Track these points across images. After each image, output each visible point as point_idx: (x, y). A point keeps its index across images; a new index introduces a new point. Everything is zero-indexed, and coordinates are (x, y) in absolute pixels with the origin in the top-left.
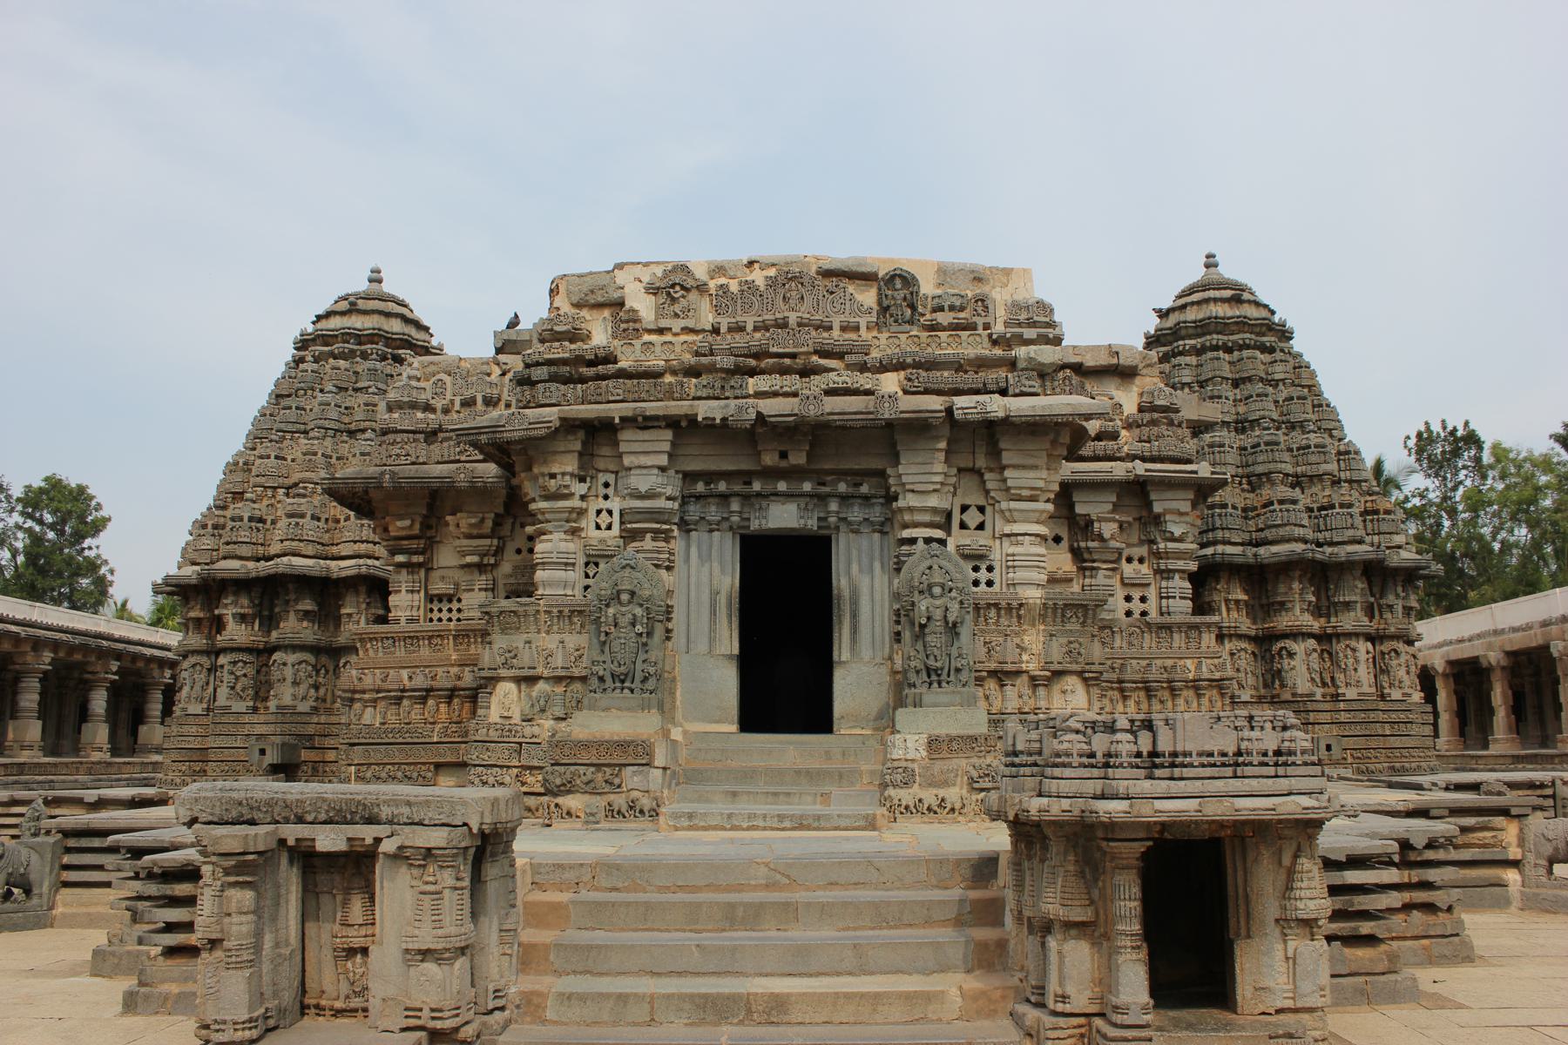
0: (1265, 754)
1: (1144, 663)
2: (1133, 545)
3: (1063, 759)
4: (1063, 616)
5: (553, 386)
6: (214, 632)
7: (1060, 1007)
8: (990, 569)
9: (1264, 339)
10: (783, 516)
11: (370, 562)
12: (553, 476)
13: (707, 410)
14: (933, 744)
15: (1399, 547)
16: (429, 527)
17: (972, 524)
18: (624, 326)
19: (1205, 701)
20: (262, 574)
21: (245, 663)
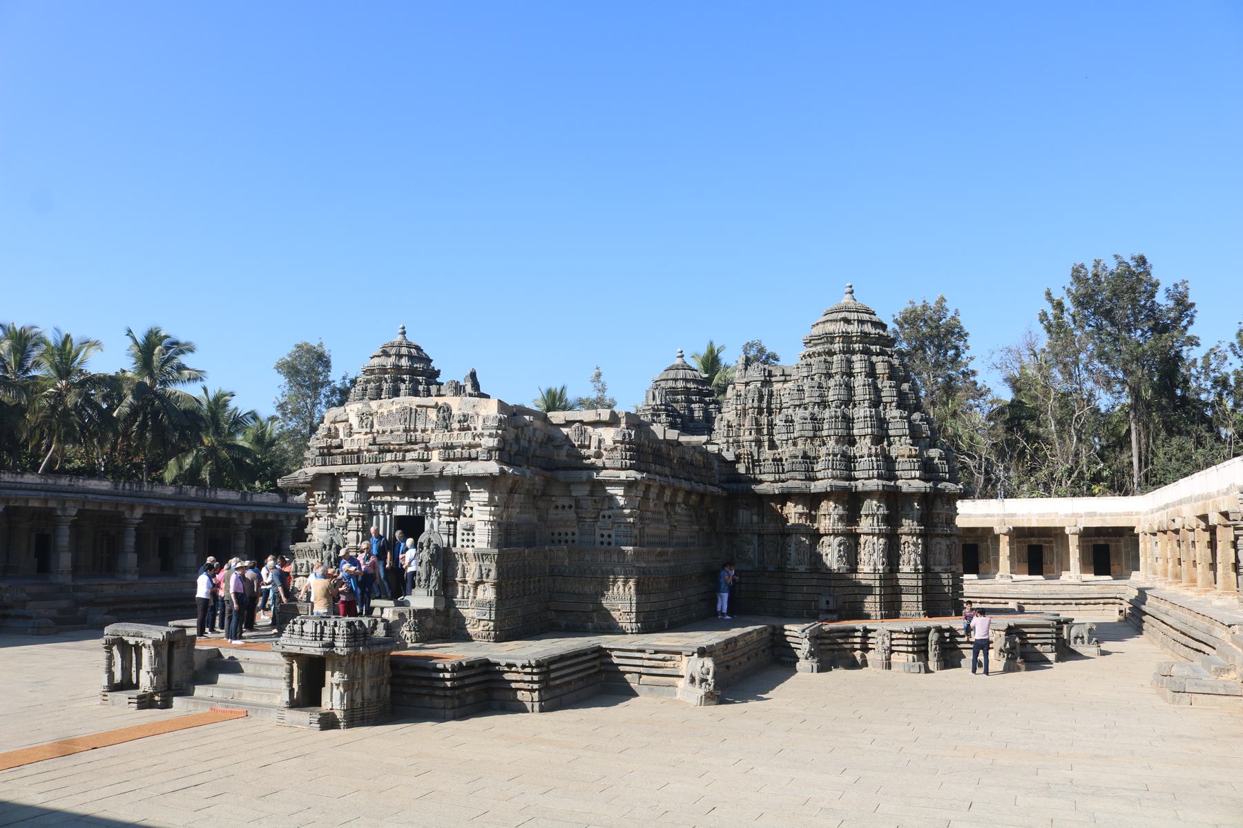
2: (604, 510)
4: (483, 559)
5: (320, 458)
8: (474, 534)
9: (857, 345)
10: (401, 511)
12: (319, 495)
17: (468, 515)
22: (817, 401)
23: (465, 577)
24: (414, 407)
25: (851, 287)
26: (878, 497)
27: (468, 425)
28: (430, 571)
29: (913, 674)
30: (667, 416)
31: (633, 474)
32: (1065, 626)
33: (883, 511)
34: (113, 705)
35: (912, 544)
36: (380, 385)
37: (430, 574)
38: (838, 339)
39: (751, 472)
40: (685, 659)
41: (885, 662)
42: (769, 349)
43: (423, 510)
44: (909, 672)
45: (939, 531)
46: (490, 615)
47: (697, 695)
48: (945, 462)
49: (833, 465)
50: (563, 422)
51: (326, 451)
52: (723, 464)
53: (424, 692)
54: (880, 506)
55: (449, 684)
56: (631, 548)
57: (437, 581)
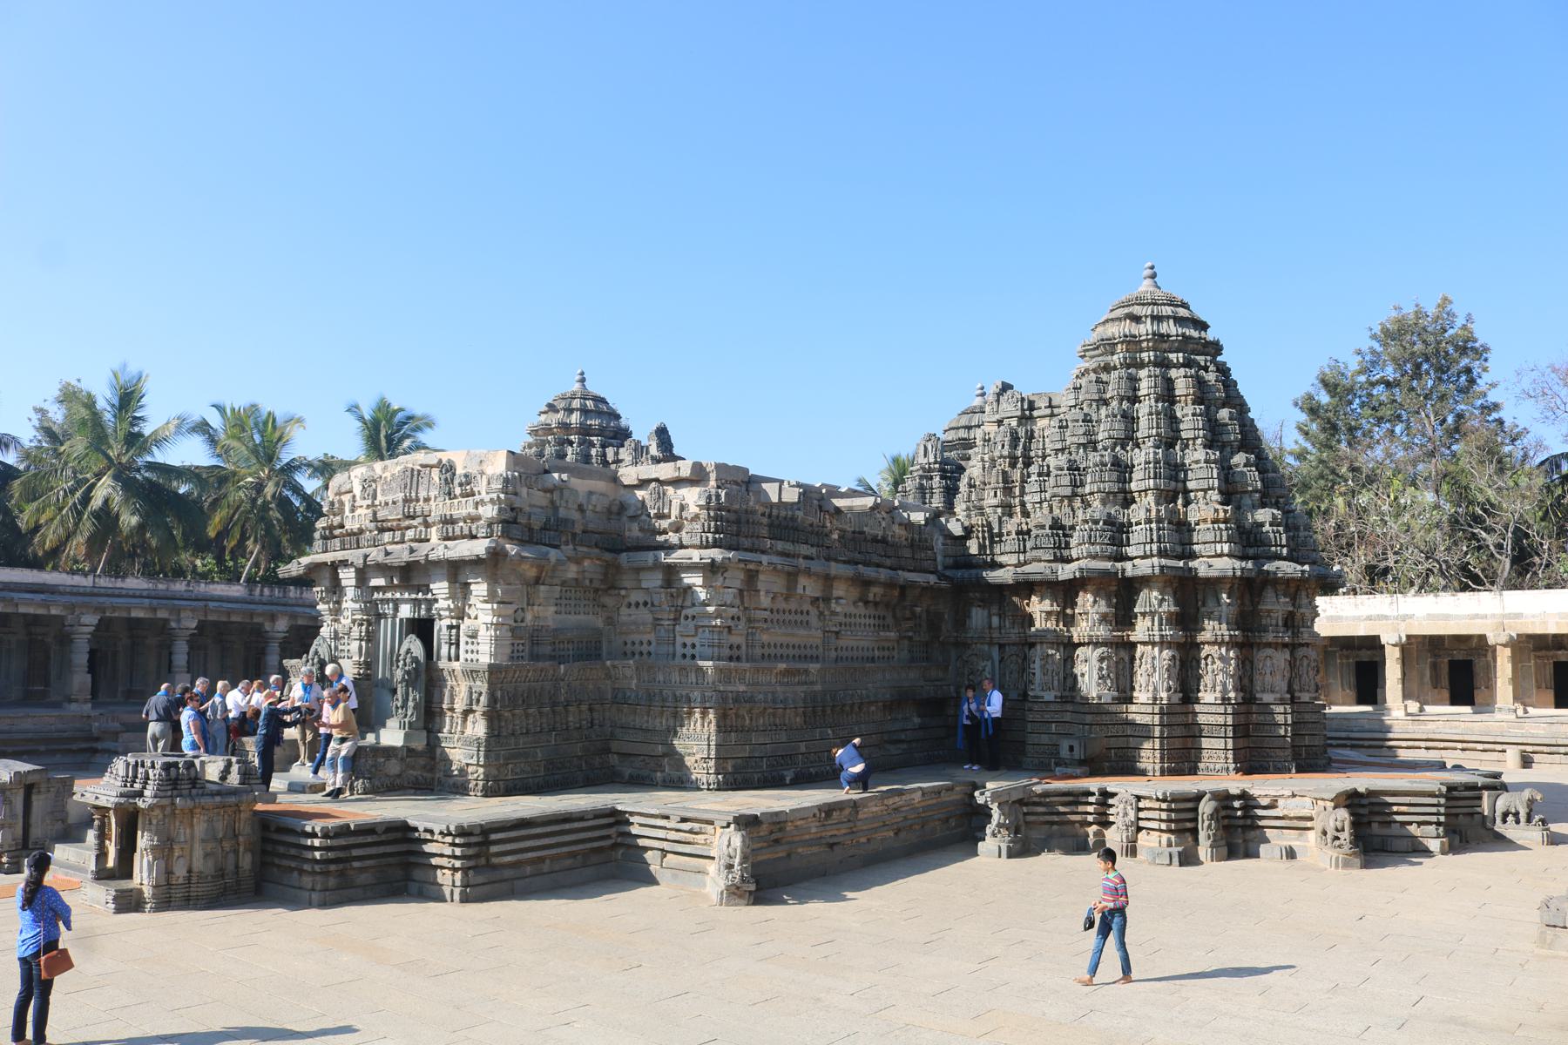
10: (405, 611)
22: (1083, 440)
25: (1152, 268)
26: (1160, 585)
27: (472, 489)
28: (407, 694)
29: (1159, 867)
30: (942, 478)
31: (717, 554)
32: (1486, 794)
35: (1219, 659)
37: (408, 700)
38: (1119, 346)
39: (988, 552)
40: (719, 831)
41: (1125, 845)
43: (429, 610)
44: (1153, 862)
45: (1270, 637)
46: (478, 758)
48: (1281, 529)
49: (1090, 537)
50: (636, 482)
51: (327, 532)
52: (949, 541)
53: (293, 864)
54: (1163, 600)
55: (317, 855)
56: (710, 663)
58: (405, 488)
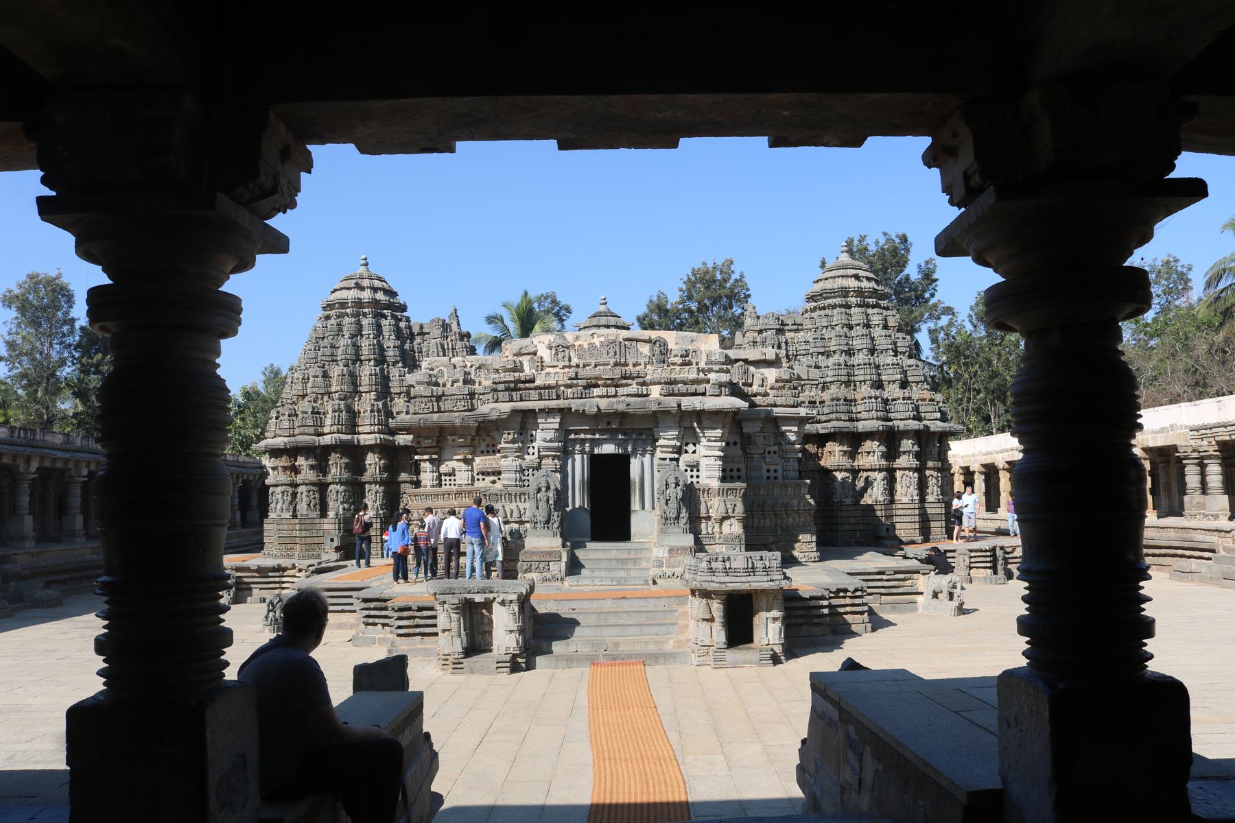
0: (765, 568)
1: (773, 502)
3: (703, 570)
4: (727, 493)
5: (507, 393)
6: (293, 474)
7: (702, 644)
8: (698, 471)
9: (872, 300)
10: (608, 449)
11: (382, 436)
12: (509, 434)
13: (575, 405)
14: (671, 551)
15: (936, 419)
16: (440, 441)
18: (537, 364)
19: (802, 519)
20: (322, 444)
21: (314, 491)
23: (708, 513)
24: (621, 340)
33: (916, 448)
34: (472, 672)
36: (359, 320)
38: (852, 293)
42: (563, 300)
47: (950, 608)
53: (800, 621)
57: (689, 518)
58: (615, 354)
